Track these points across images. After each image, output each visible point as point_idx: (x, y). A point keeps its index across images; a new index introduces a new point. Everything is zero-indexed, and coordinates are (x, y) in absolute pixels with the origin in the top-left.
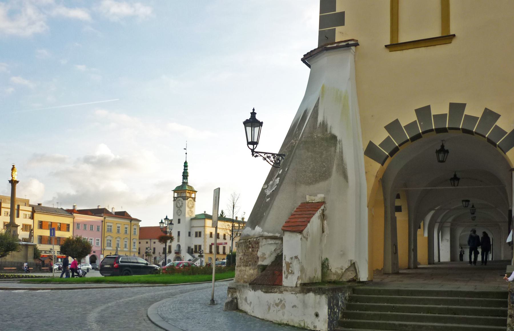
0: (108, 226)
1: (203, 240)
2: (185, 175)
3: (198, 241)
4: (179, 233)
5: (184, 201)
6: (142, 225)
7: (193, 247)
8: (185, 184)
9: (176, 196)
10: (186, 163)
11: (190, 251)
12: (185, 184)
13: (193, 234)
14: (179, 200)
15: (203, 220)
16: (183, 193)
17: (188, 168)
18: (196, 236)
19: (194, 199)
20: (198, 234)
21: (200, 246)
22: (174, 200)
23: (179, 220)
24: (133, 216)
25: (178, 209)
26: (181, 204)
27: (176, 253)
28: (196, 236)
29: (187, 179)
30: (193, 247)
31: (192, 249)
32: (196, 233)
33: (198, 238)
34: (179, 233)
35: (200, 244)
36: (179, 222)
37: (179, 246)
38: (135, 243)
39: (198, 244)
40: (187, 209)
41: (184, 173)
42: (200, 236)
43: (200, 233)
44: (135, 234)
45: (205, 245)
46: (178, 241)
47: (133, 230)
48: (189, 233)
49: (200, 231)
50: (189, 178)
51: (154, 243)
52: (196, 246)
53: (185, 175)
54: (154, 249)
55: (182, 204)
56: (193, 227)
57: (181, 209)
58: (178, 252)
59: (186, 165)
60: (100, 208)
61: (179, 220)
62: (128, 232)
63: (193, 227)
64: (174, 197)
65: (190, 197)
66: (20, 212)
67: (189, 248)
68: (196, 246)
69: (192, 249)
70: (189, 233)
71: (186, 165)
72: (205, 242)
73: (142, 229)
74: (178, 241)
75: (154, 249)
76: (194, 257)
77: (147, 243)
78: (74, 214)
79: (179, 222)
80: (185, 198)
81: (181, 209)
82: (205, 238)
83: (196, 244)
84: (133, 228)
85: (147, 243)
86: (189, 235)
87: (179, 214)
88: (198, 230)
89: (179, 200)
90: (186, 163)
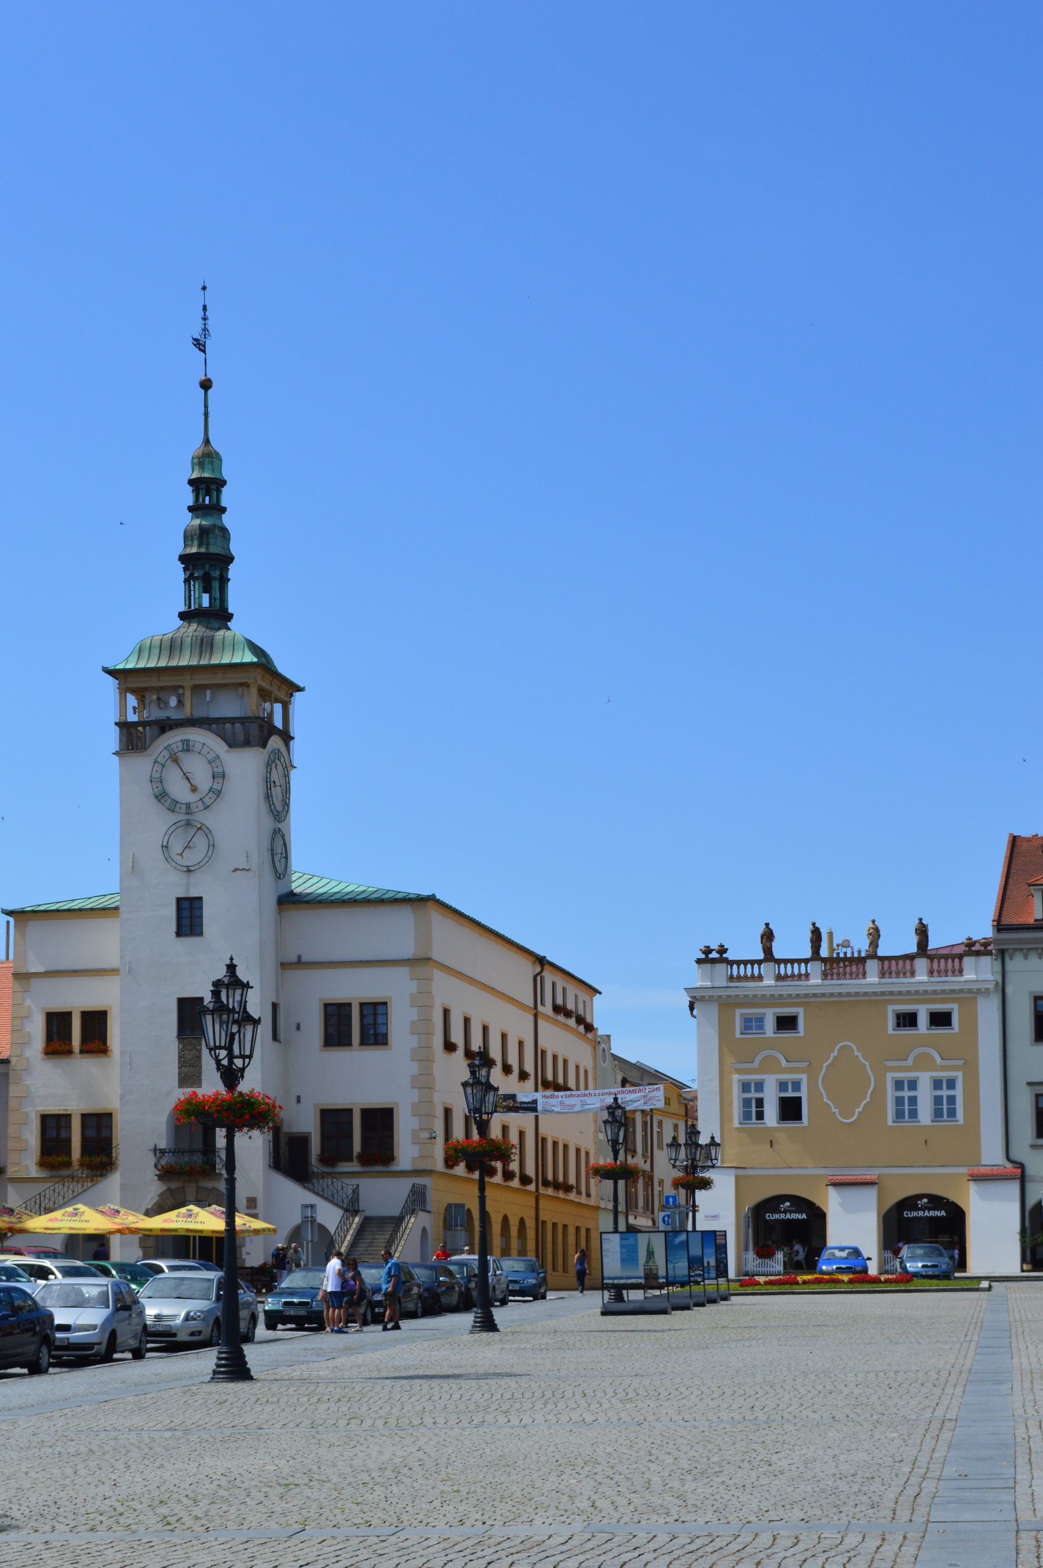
2: (207, 564)
10: (208, 457)
14: (187, 747)
26: (204, 782)
35: (376, 1100)
42: (375, 1035)
43: (375, 1012)
49: (372, 994)
50: (234, 571)
52: (334, 1119)
53: (207, 564)
55: (219, 776)
56: (300, 963)
63: (300, 963)
64: (123, 726)
69: (300, 1142)
72: (424, 1082)
83: (338, 1100)
87: (191, 858)
88: (354, 988)
89: (187, 747)
90: (208, 457)
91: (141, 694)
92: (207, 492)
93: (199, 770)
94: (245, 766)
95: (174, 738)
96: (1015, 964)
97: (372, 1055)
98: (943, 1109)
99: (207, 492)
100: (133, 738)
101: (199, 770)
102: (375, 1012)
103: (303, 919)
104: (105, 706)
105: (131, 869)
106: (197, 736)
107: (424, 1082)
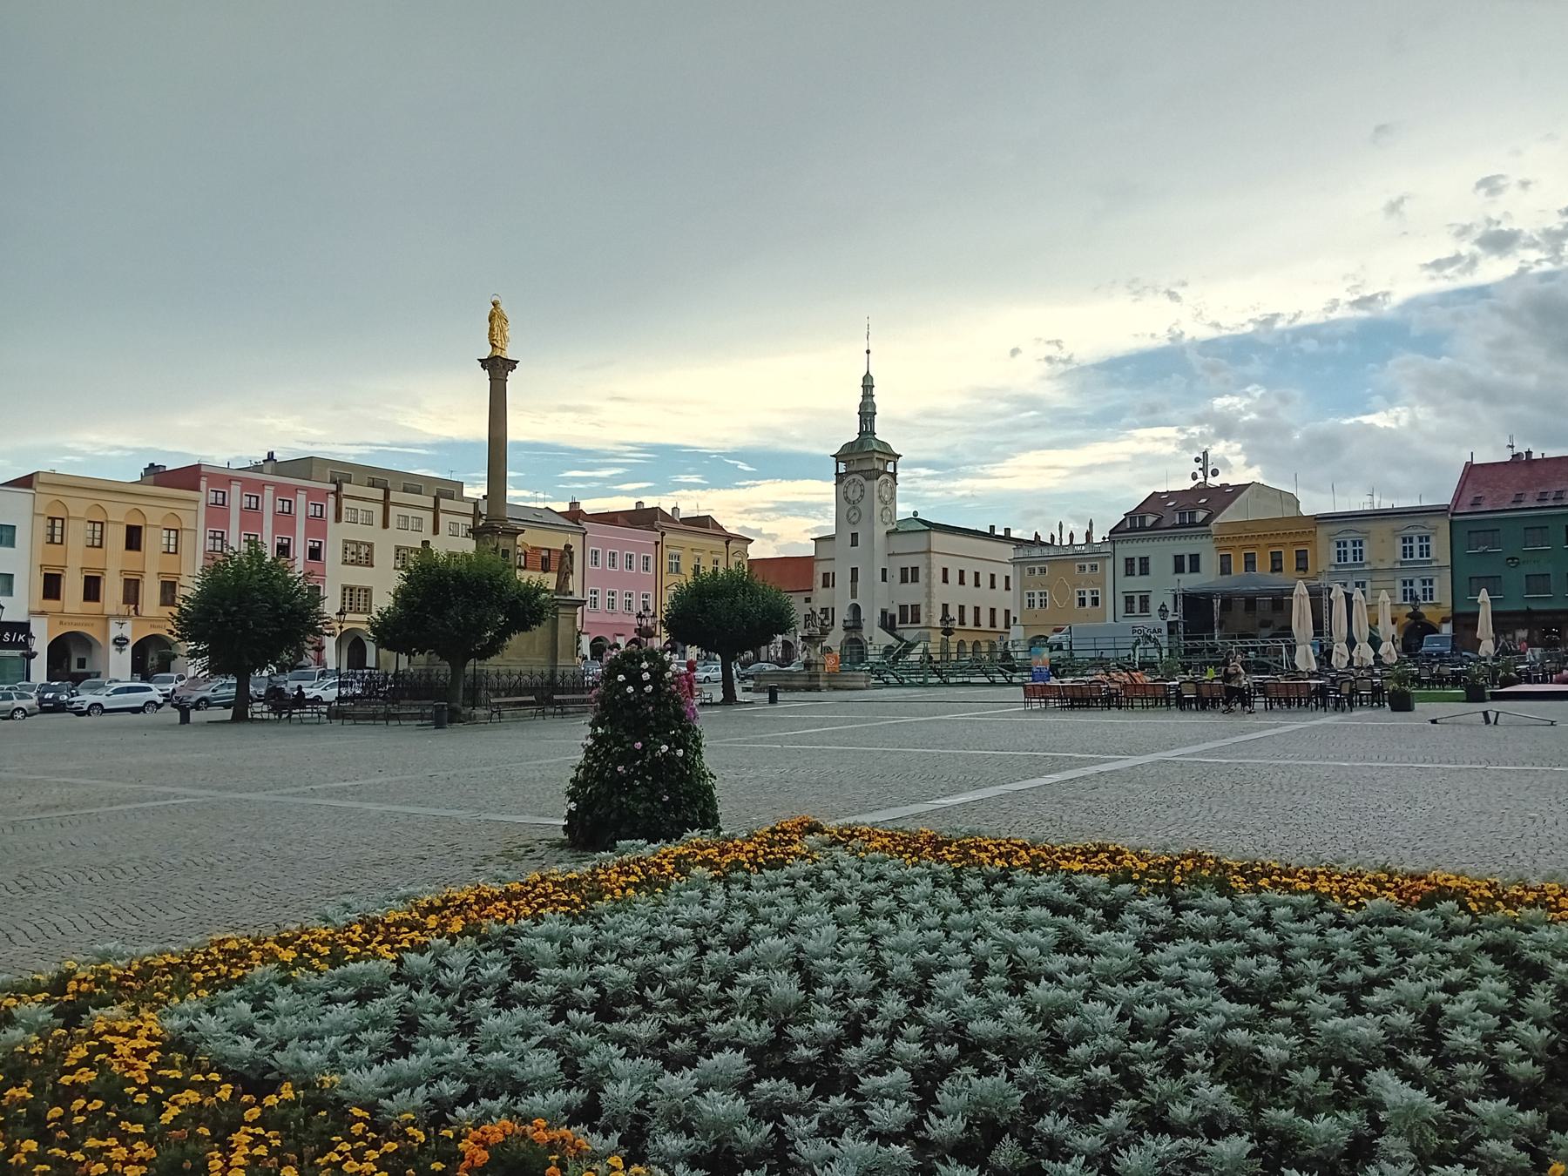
0: (671, 557)
2: (867, 413)
3: (910, 594)
4: (855, 571)
5: (867, 484)
9: (842, 470)
11: (888, 623)
15: (924, 535)
16: (864, 462)
18: (904, 580)
19: (894, 475)
20: (909, 575)
21: (916, 608)
23: (855, 536)
25: (850, 506)
27: (846, 629)
28: (904, 580)
29: (872, 421)
30: (896, 612)
31: (893, 617)
32: (904, 570)
33: (910, 586)
34: (855, 571)
36: (854, 543)
37: (856, 609)
39: (909, 602)
40: (878, 506)
42: (915, 580)
43: (915, 570)
45: (929, 606)
46: (854, 596)
52: (903, 608)
53: (867, 413)
57: (860, 506)
58: (854, 623)
59: (868, 385)
61: (855, 536)
66: (441, 515)
67: (884, 613)
68: (903, 608)
69: (893, 617)
71: (868, 385)
72: (929, 595)
74: (854, 596)
76: (901, 639)
78: (586, 525)
79: (854, 543)
80: (873, 475)
81: (860, 506)
82: (929, 585)
87: (855, 519)
88: (909, 562)
95: (850, 478)
97: (915, 585)
98: (1095, 601)
102: (915, 570)
103: (894, 538)
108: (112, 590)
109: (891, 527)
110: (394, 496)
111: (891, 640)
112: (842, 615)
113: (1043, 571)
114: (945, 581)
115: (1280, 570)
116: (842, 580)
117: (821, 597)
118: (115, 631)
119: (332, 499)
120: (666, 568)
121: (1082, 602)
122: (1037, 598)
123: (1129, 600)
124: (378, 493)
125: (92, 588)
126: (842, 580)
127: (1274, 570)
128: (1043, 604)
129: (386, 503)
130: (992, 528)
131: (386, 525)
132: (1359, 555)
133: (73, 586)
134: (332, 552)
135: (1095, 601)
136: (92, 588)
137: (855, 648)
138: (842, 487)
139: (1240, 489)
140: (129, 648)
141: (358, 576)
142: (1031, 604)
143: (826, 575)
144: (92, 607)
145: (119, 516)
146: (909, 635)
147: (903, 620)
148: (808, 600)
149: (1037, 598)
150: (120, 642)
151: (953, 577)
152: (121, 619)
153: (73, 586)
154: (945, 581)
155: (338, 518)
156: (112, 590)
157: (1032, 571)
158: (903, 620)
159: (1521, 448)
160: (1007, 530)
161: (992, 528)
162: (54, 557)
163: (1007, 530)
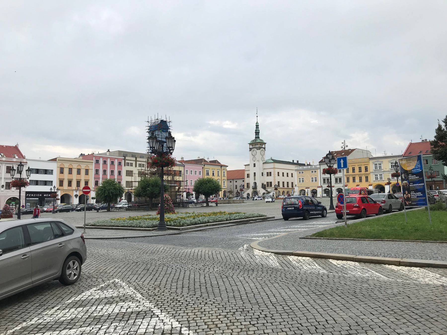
0: (207, 171)
1: (273, 178)
2: (257, 133)
3: (269, 179)
4: (255, 173)
6: (228, 169)
7: (265, 183)
8: (257, 137)
10: (257, 123)
11: (264, 187)
12: (257, 137)
13: (265, 174)
16: (257, 144)
17: (259, 127)
18: (268, 175)
19: (265, 148)
20: (269, 174)
21: (271, 183)
22: (250, 150)
24: (222, 163)
27: (253, 188)
29: (258, 134)
30: (265, 183)
31: (265, 185)
32: (268, 173)
33: (269, 177)
34: (255, 173)
36: (255, 166)
37: (255, 183)
38: (224, 182)
39: (269, 181)
41: (256, 130)
42: (270, 175)
43: (270, 173)
44: (224, 176)
45: (275, 182)
46: (255, 180)
47: (223, 173)
48: (262, 173)
51: (236, 182)
52: (268, 183)
53: (257, 133)
54: (236, 186)
60: (200, 158)
62: (220, 175)
65: (262, 148)
67: (263, 184)
68: (268, 183)
69: (265, 185)
70: (262, 173)
72: (275, 179)
73: (230, 173)
74: (255, 180)
75: (236, 186)
76: (267, 191)
77: (231, 182)
79: (255, 166)
81: (256, 156)
82: (274, 177)
84: (223, 171)
85: (231, 182)
86: (262, 175)
88: (269, 171)
91: (252, 145)
92: (257, 126)
93: (255, 152)
94: (259, 151)
95: (253, 149)
96: (321, 166)
98: (316, 180)
99: (257, 126)
100: (251, 149)
101: (255, 152)
104: (248, 146)
105: (250, 161)
106: (255, 149)
107: (275, 179)
108: (74, 184)
109: (264, 162)
110: (138, 159)
111: (264, 191)
112: (252, 185)
113: (302, 173)
114: (278, 175)
115: (361, 171)
116: (252, 175)
117: (247, 180)
118: (75, 193)
119: (123, 161)
120: (205, 174)
121: (312, 181)
122: (301, 180)
123: (324, 180)
124: (134, 159)
125: (70, 183)
126: (252, 175)
127: (359, 172)
128: (303, 181)
129: (136, 161)
130: (293, 161)
131: (136, 166)
132: (380, 167)
133: (66, 183)
134: (124, 173)
135: (316, 180)
136: (70, 183)
137: (255, 193)
138: (251, 152)
139: (353, 150)
140: (78, 197)
141: (129, 179)
142: (300, 181)
143: (248, 175)
144: (70, 188)
145: (75, 166)
146: (269, 190)
147: (268, 186)
148: (243, 181)
149: (301, 180)
150: (76, 196)
151: (281, 174)
152: (76, 190)
153: (66, 183)
154: (278, 175)
155: (125, 165)
156: (74, 184)
157: (300, 173)
158: (268, 186)
159: (424, 139)
160: (298, 161)
161: (293, 161)
162: (62, 176)
163: (298, 161)
